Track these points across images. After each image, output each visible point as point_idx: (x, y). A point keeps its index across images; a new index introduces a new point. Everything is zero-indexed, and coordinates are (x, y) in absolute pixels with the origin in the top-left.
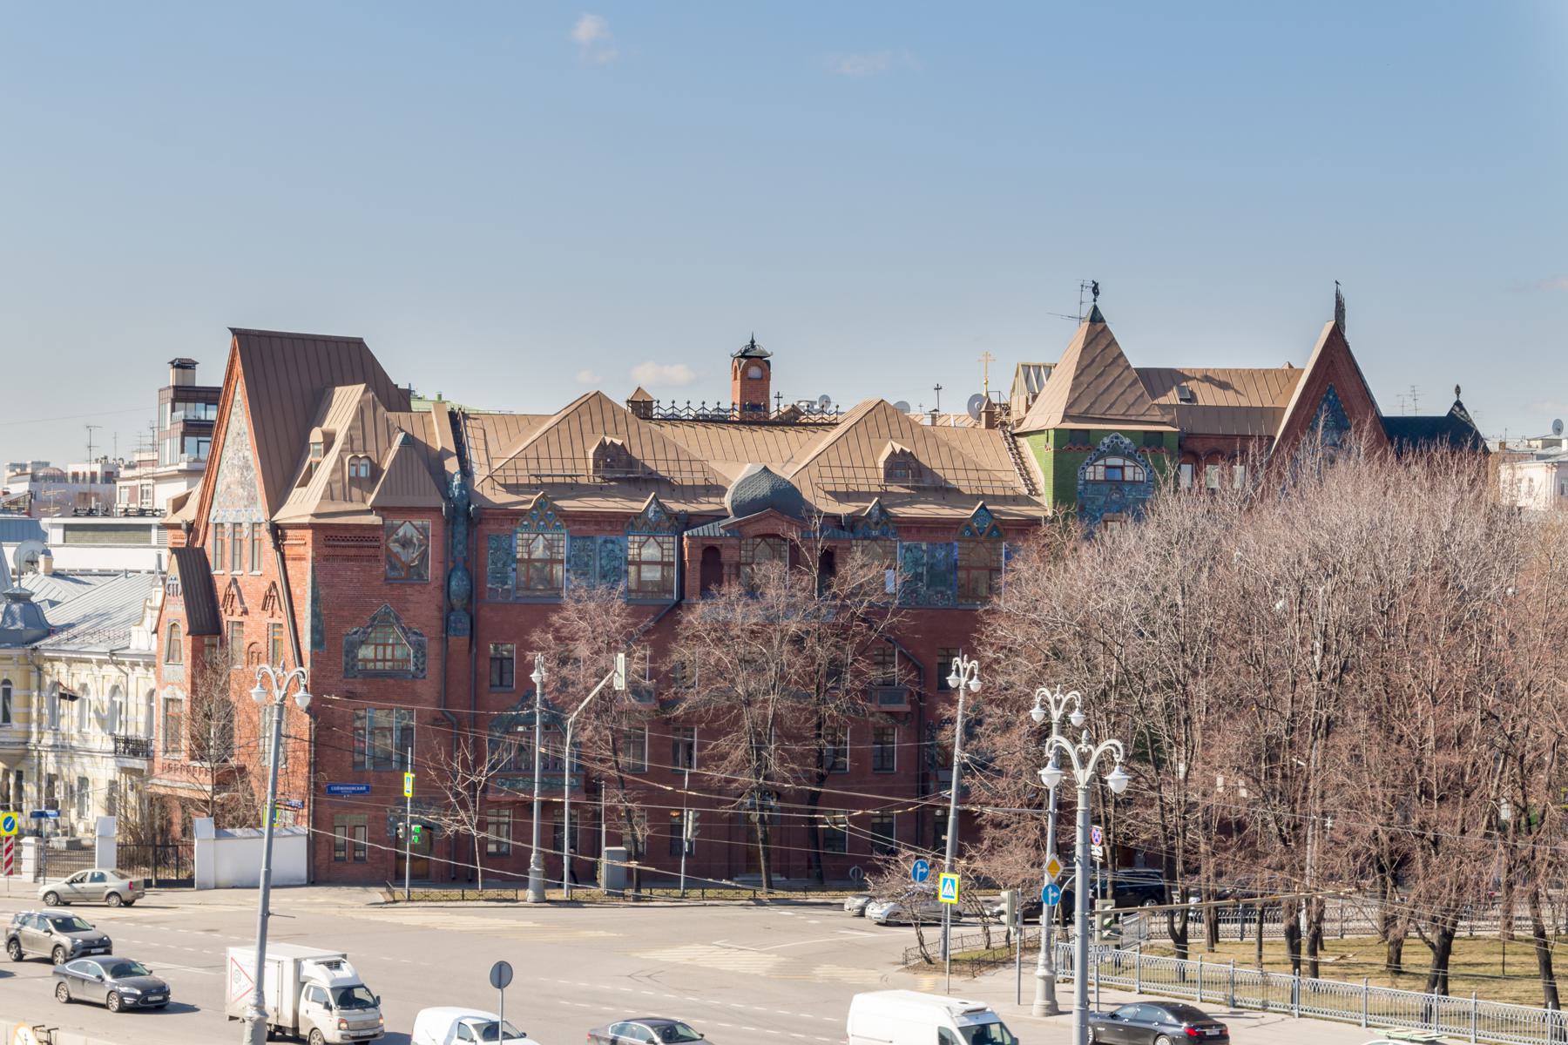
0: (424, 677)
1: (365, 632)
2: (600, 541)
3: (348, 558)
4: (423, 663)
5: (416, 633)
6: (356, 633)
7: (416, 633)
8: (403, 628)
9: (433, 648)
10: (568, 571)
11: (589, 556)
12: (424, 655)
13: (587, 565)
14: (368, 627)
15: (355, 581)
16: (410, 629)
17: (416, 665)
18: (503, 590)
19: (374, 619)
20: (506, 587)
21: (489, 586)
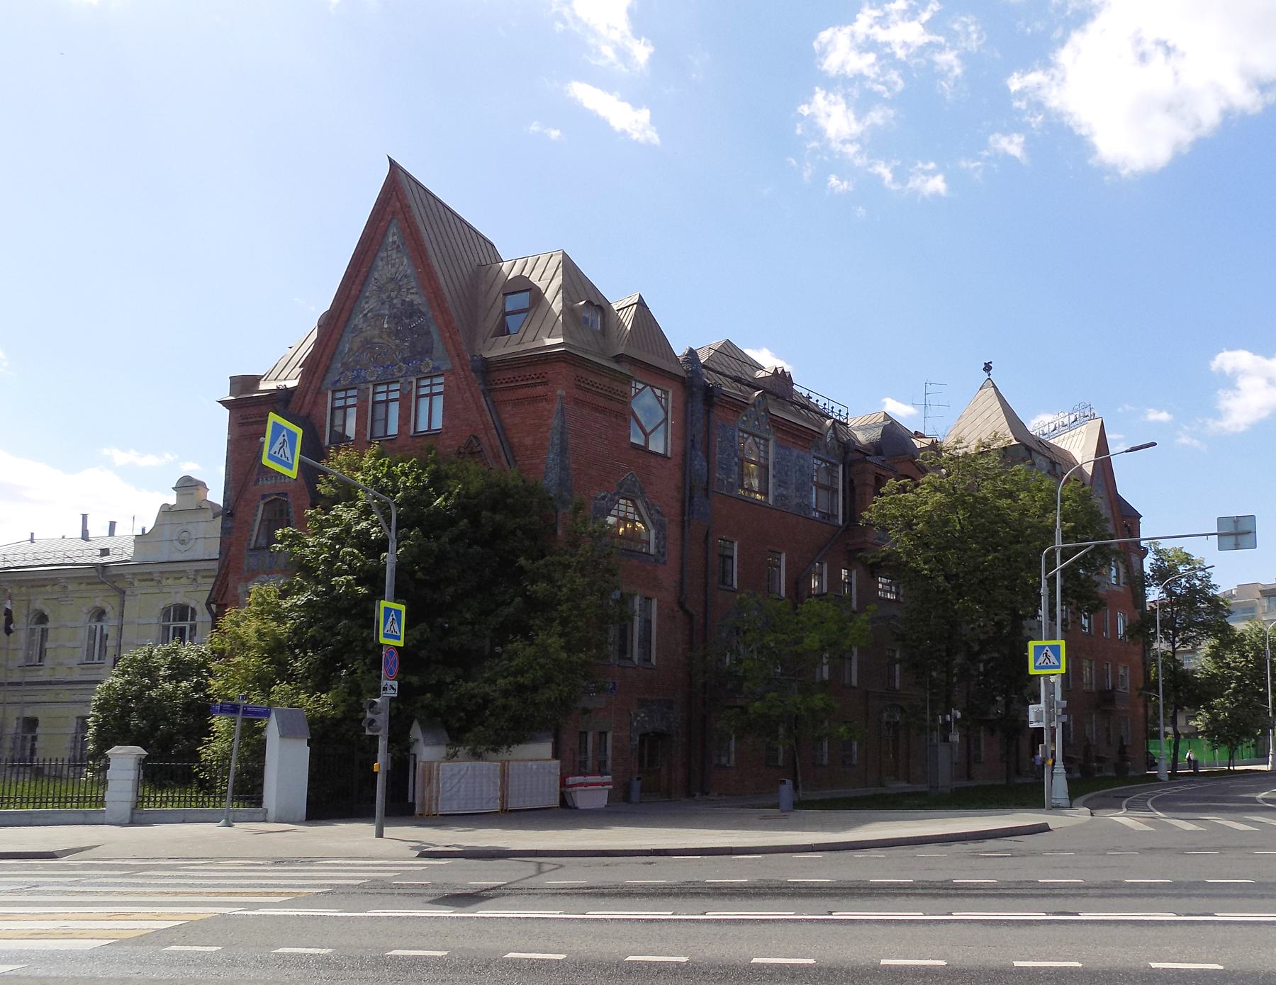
0: (665, 563)
1: (611, 500)
2: (795, 454)
3: (596, 408)
4: (664, 547)
5: (658, 512)
6: (603, 498)
7: (658, 512)
8: (646, 502)
9: (673, 531)
10: (774, 476)
11: (788, 466)
12: (665, 538)
13: (786, 474)
14: (615, 494)
15: (604, 436)
16: (653, 505)
17: (657, 547)
18: (728, 482)
19: (621, 486)
20: (730, 480)
21: (717, 475)
